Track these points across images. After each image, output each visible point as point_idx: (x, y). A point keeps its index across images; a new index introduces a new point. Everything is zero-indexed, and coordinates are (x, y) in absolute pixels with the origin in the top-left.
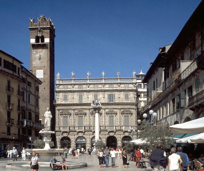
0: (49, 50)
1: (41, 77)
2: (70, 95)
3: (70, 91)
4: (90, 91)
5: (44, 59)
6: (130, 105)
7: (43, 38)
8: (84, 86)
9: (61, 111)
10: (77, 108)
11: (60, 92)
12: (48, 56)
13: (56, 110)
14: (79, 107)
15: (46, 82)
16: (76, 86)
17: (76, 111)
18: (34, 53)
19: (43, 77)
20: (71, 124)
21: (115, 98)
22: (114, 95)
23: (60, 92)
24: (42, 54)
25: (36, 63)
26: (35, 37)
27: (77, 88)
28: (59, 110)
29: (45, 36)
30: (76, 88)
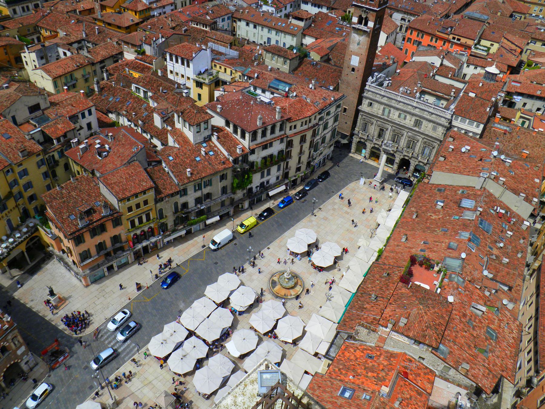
2: (376, 105)
3: (377, 101)
11: (367, 98)
21: (421, 125)
22: (422, 122)
25: (353, 47)
29: (370, 19)
30: (385, 100)
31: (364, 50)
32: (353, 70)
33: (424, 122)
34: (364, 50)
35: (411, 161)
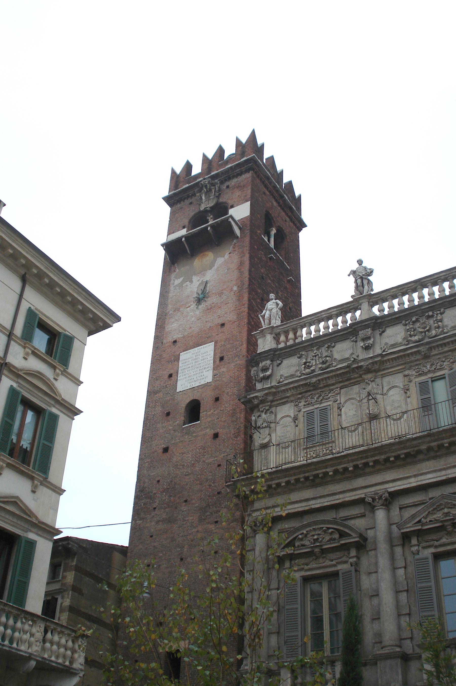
0: (247, 250)
1: (203, 383)
3: (352, 374)
5: (220, 294)
10: (413, 482)
12: (241, 273)
15: (224, 398)
16: (390, 331)
18: (178, 282)
19: (210, 379)
24: (209, 276)
29: (230, 202)
32: (194, 410)
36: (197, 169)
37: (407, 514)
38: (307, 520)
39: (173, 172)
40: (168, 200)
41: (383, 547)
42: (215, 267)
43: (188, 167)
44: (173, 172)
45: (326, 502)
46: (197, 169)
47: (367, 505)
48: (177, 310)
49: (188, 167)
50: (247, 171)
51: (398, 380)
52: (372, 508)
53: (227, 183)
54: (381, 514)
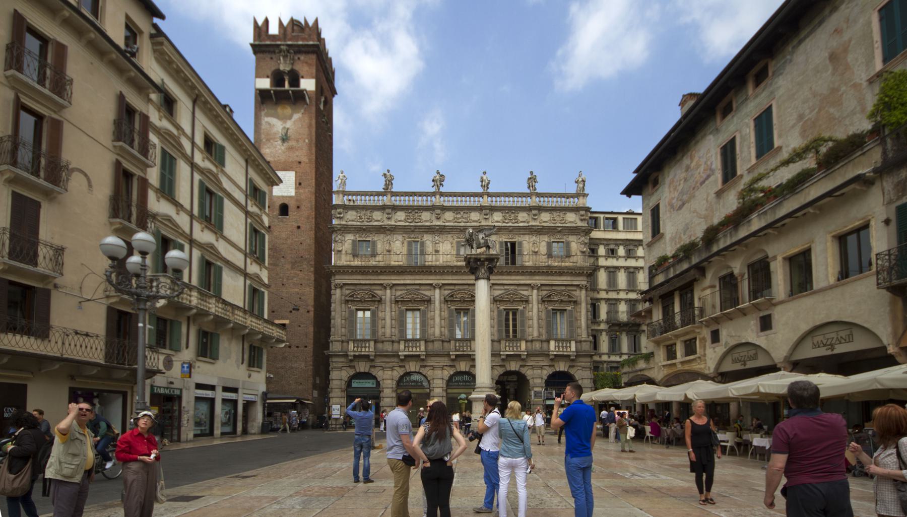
0: (314, 115)
2: (381, 243)
4: (442, 230)
5: (297, 141)
6: (571, 274)
7: (295, 80)
8: (426, 216)
9: (348, 292)
10: (402, 282)
12: (311, 132)
13: (333, 287)
14: (408, 280)
17: (398, 293)
18: (267, 119)
19: (293, 194)
20: (380, 333)
21: (521, 254)
22: (520, 243)
23: (346, 229)
24: (289, 124)
26: (269, 73)
27: (400, 221)
28: (342, 286)
29: (301, 74)
31: (305, 149)
33: (527, 243)
34: (304, 153)
35: (528, 373)
36: (274, 30)
37: (398, 293)
38: (358, 287)
39: (255, 22)
40: (252, 45)
41: (388, 303)
42: (293, 120)
43: (266, 21)
44: (255, 22)
45: (367, 282)
46: (274, 30)
47: (384, 287)
48: (268, 140)
49: (266, 21)
50: (313, 52)
51: (400, 237)
52: (385, 288)
53: (299, 56)
54: (388, 291)
